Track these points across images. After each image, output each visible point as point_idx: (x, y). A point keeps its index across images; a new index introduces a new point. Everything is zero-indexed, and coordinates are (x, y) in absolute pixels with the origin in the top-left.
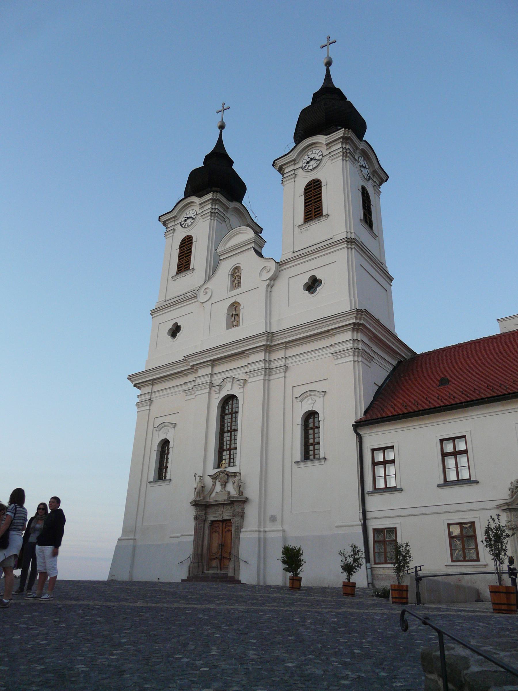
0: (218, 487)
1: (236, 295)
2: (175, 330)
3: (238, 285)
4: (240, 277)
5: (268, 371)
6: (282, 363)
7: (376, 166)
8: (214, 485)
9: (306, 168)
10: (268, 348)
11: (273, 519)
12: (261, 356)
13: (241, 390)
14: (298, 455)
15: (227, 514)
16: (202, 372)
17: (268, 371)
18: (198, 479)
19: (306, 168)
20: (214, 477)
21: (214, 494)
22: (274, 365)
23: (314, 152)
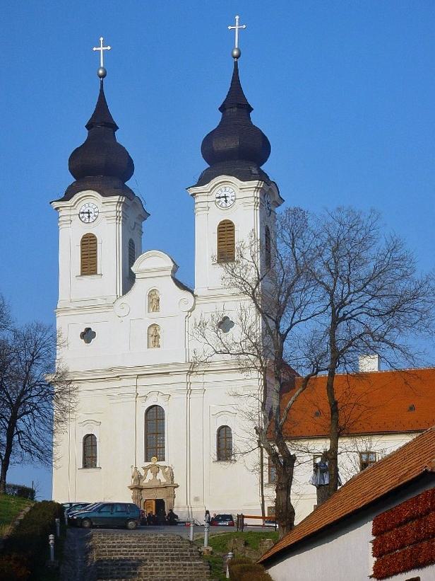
0: (150, 476)
1: (154, 318)
2: (88, 335)
3: (156, 309)
4: (158, 300)
5: (190, 391)
6: (199, 386)
7: (277, 196)
8: (146, 474)
9: (220, 204)
10: (190, 372)
11: (197, 499)
12: (183, 378)
13: (167, 403)
14: (216, 458)
15: (160, 495)
16: (125, 382)
17: (190, 391)
18: (134, 470)
19: (220, 204)
20: (144, 468)
21: (146, 481)
22: (192, 387)
23: (227, 189)
